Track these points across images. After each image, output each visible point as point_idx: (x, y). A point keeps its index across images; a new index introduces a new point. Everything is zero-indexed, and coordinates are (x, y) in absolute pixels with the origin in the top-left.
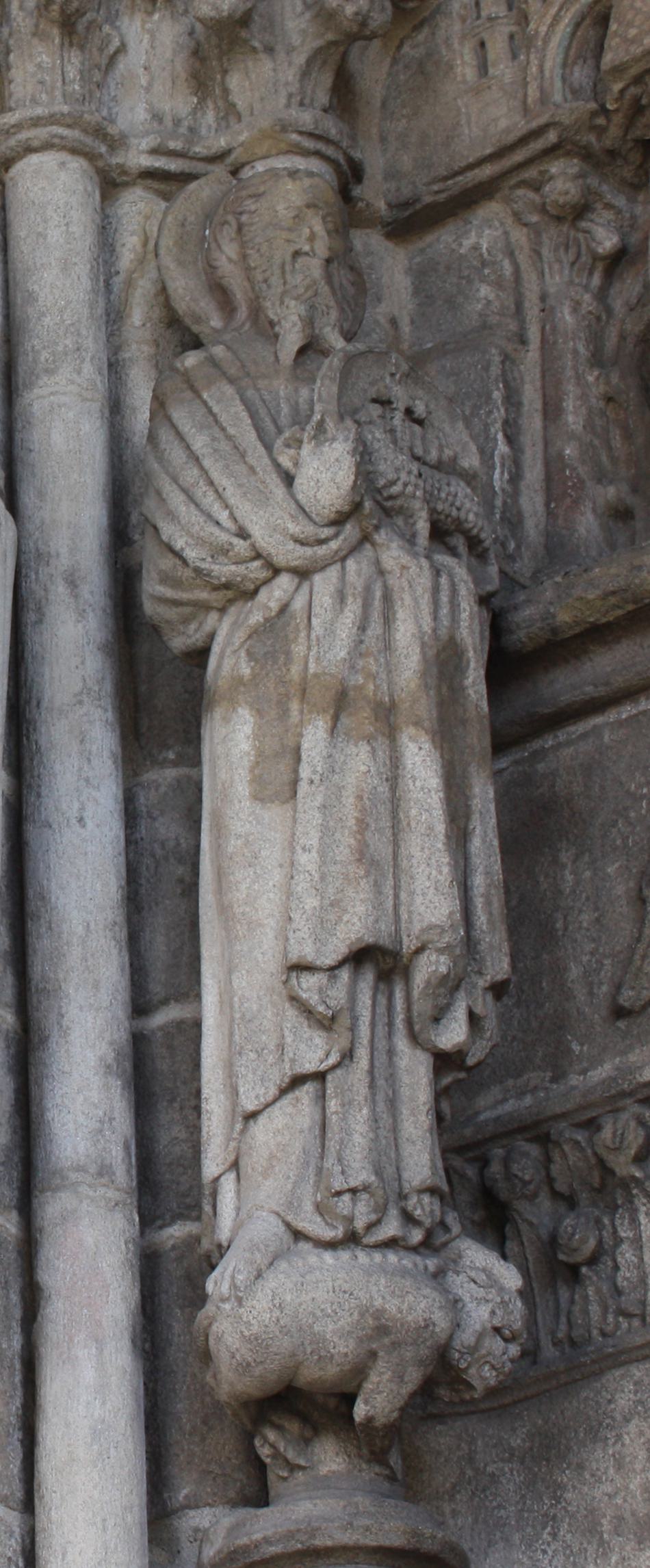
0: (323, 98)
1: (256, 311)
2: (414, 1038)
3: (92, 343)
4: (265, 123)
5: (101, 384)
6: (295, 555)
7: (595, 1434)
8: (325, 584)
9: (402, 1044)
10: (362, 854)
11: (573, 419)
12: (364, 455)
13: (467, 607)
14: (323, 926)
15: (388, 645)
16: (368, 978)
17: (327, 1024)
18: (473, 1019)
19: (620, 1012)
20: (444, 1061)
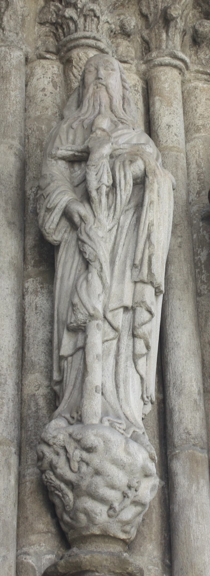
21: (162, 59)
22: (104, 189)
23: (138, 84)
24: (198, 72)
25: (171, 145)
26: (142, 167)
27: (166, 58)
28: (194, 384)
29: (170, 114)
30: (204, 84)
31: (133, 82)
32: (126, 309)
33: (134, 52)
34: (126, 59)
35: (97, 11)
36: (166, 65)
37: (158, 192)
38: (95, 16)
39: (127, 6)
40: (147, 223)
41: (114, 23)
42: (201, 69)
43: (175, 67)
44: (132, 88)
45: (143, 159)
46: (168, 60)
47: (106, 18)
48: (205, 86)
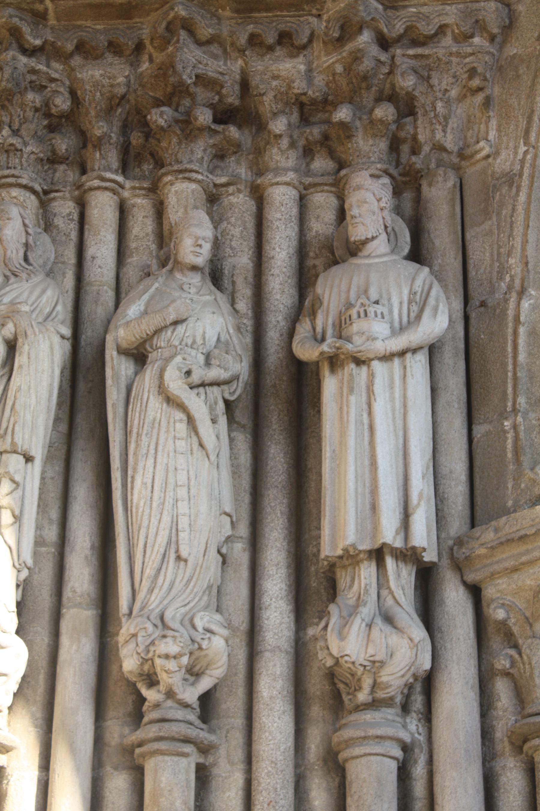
21: (91, 183)
23: (74, 211)
24: (134, 188)
25: (93, 280)
26: (13, 330)
27: (95, 181)
28: (87, 538)
29: (96, 244)
30: (143, 199)
31: (68, 211)
33: (72, 176)
34: (57, 188)
35: (17, 145)
36: (98, 188)
37: (29, 354)
38: (17, 150)
39: (65, 124)
40: (15, 388)
41: (40, 152)
42: (137, 185)
43: (106, 189)
44: (66, 218)
45: (13, 322)
46: (96, 183)
47: (31, 148)
48: (144, 201)
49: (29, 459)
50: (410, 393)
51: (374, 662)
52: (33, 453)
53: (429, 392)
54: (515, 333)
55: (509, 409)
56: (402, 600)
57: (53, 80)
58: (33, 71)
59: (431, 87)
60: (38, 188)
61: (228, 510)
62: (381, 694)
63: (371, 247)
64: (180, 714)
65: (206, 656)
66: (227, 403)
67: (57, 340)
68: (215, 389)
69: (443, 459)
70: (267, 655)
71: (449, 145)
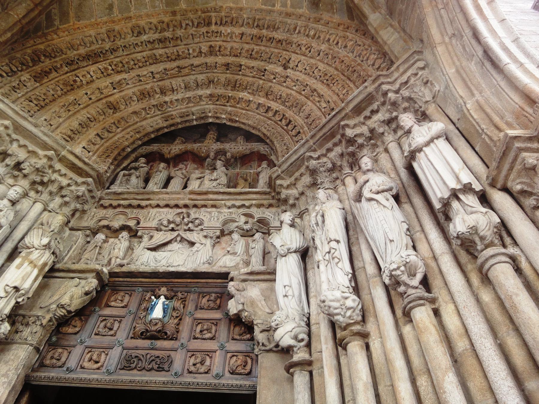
0: (71, 214)
1: (50, 226)
2: (16, 299)
3: (32, 221)
4: (64, 212)
5: (30, 225)
6: (37, 247)
7: (8, 351)
8: (38, 251)
9: (14, 298)
10: (23, 278)
11: (75, 253)
12: (50, 241)
13: (51, 261)
14: (13, 282)
15: (40, 260)
16: (15, 290)
17: (7, 292)
18: (23, 300)
19: (41, 308)
20: (17, 303)
22: (314, 225)
32: (329, 252)
36: (345, 177)
49: (338, 242)
50: (440, 148)
51: (471, 228)
52: (338, 239)
53: (454, 152)
54: (470, 114)
55: (480, 131)
56: (473, 205)
57: (325, 163)
58: (319, 163)
59: (415, 92)
60: (331, 187)
61: (403, 220)
62: (486, 242)
63: (413, 129)
64: (414, 291)
65: (412, 265)
66: (393, 196)
67: (338, 210)
68: (385, 193)
69: (470, 163)
70: (440, 257)
71: (428, 100)
